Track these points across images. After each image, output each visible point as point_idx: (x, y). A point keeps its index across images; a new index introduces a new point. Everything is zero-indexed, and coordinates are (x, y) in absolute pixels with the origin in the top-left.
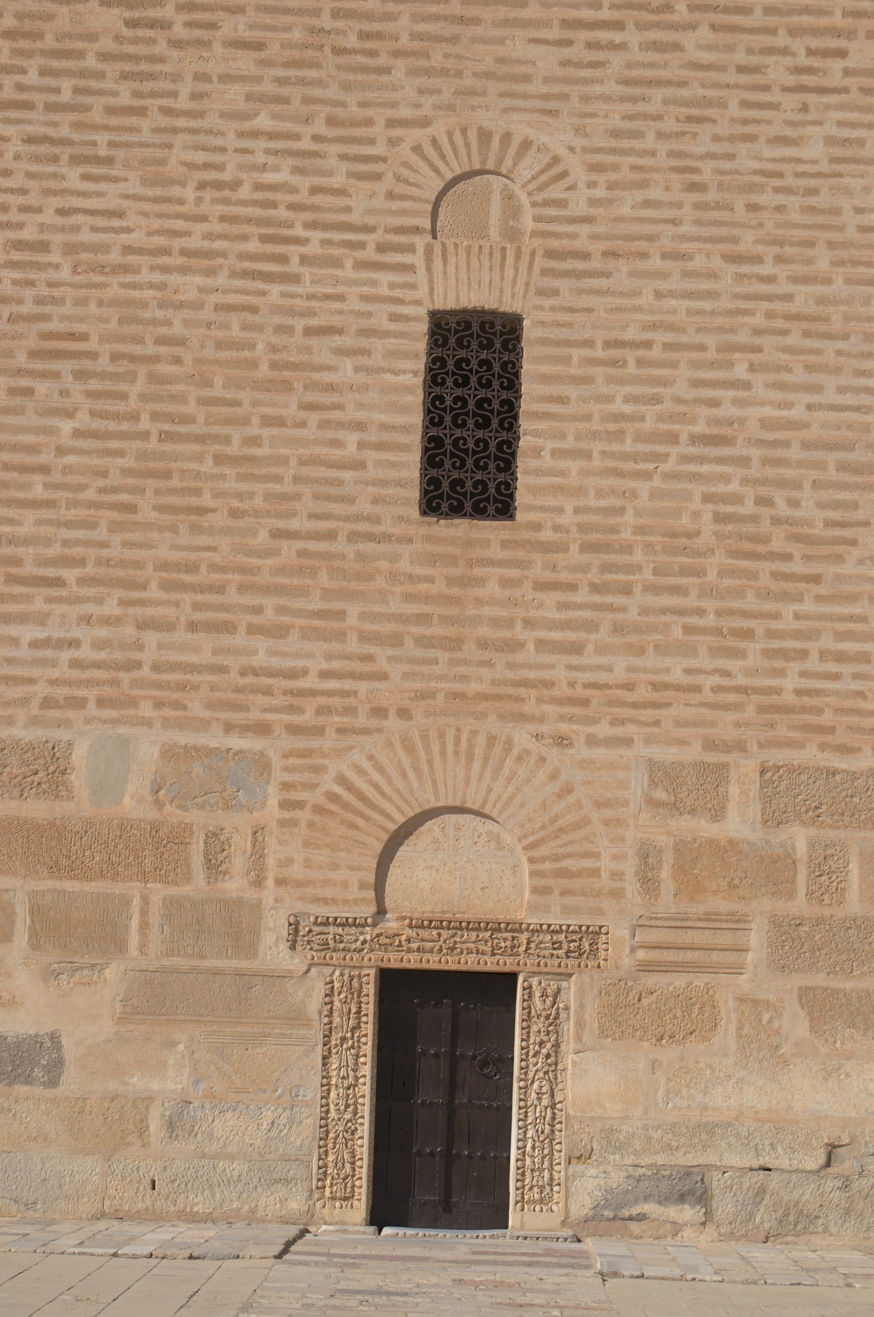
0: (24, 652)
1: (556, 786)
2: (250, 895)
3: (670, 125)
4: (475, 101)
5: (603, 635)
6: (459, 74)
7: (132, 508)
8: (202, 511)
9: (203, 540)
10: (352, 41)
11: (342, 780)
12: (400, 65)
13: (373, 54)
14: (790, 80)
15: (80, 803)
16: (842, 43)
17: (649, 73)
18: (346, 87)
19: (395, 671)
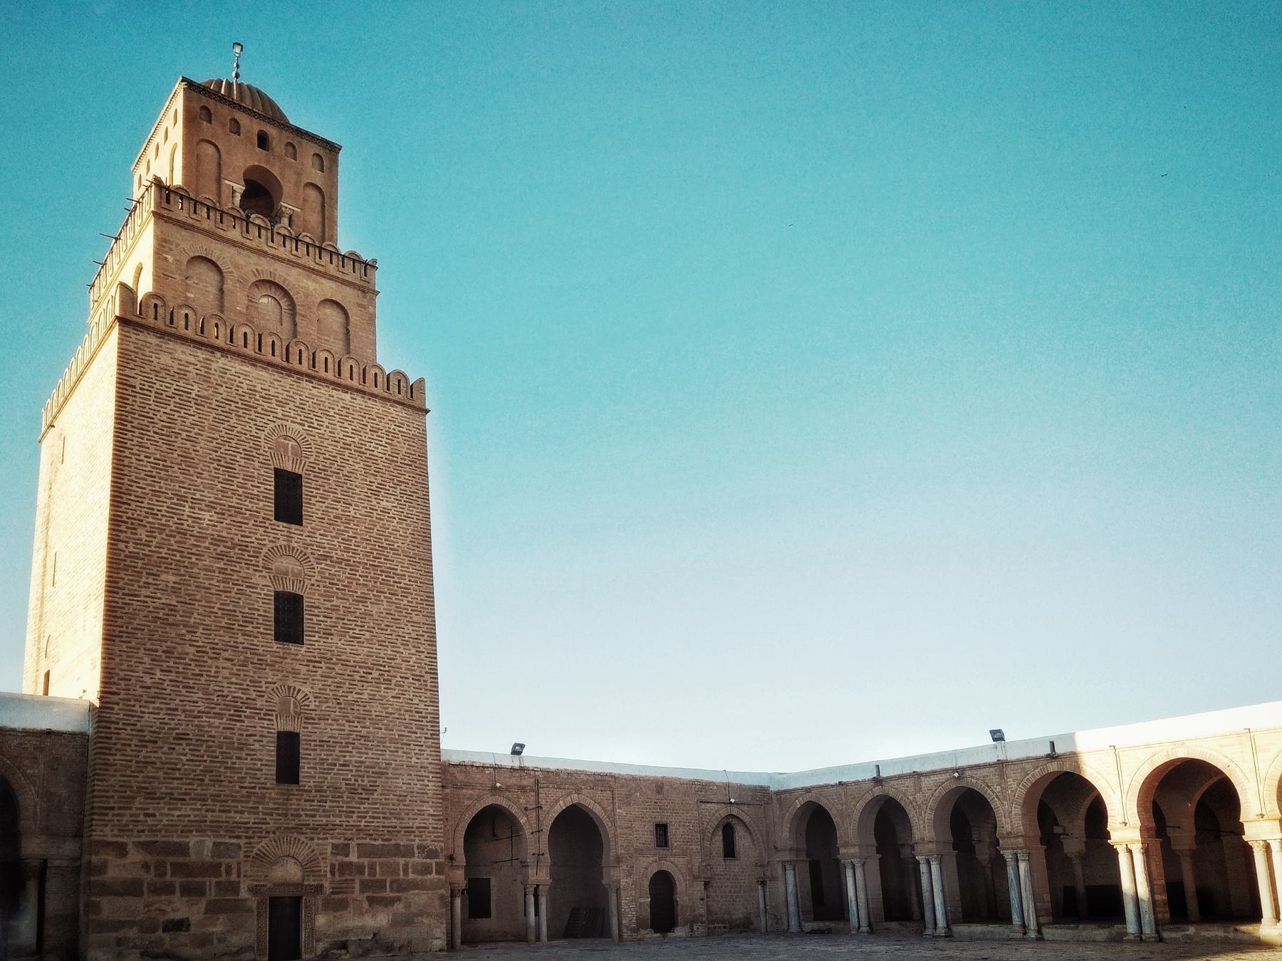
15: (193, 857)
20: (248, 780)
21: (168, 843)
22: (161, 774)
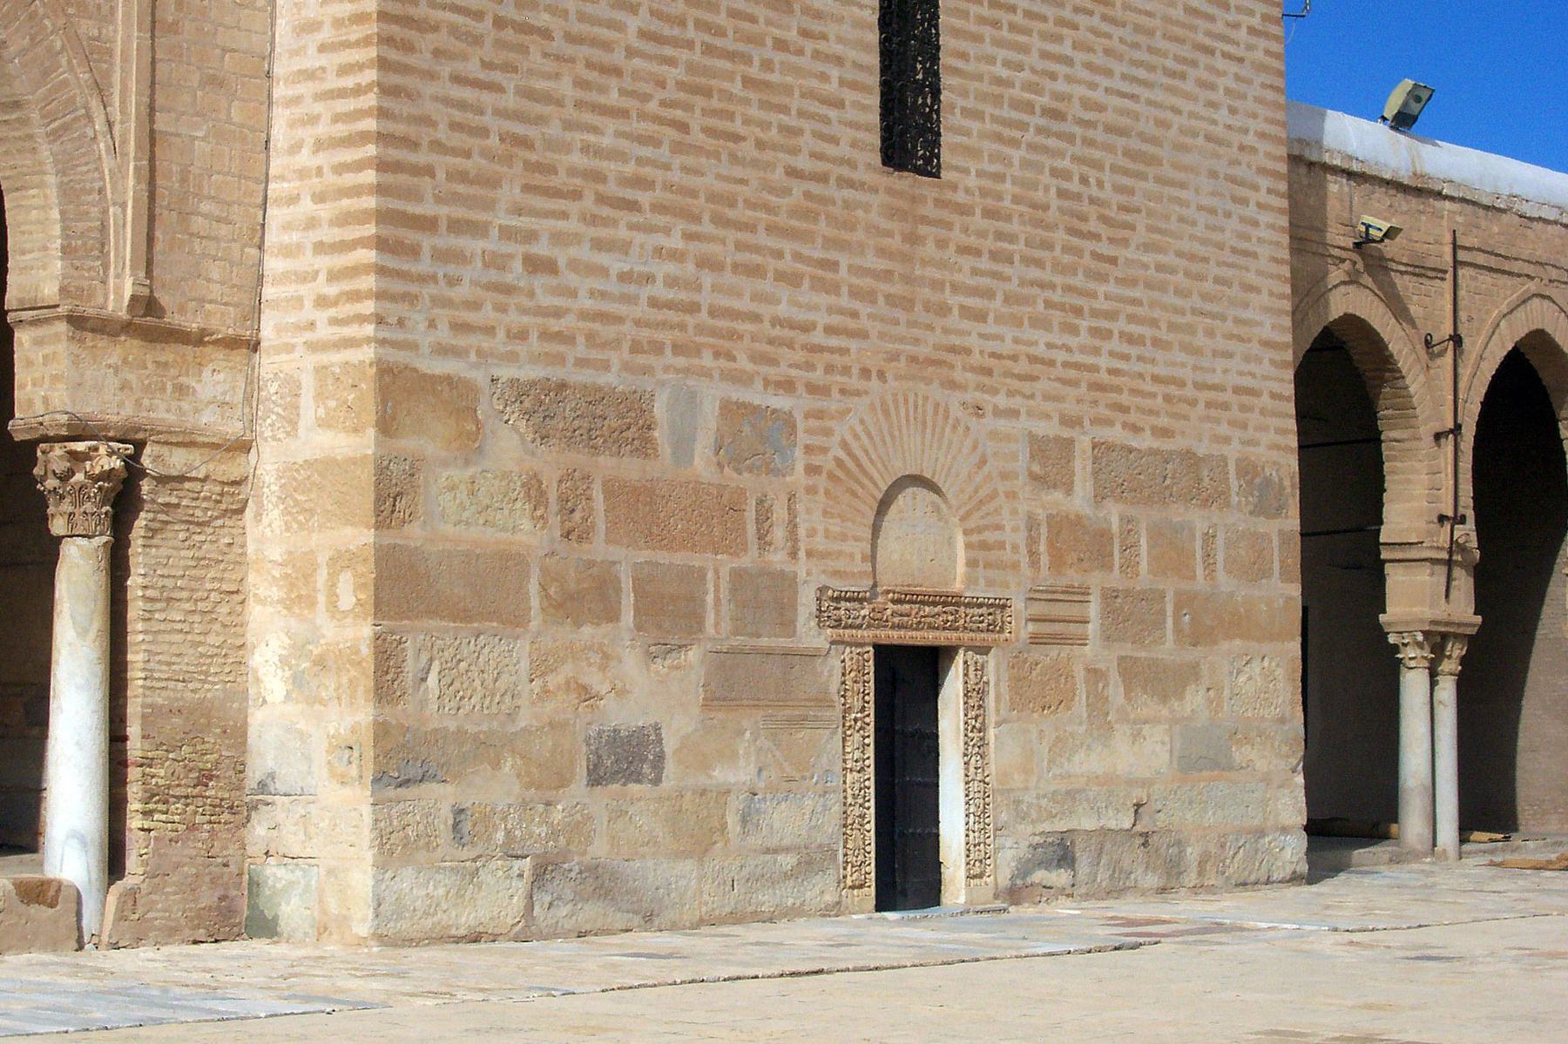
0: (613, 287)
1: (975, 458)
2: (788, 568)
5: (997, 303)
7: (683, 127)
8: (737, 138)
9: (738, 172)
11: (844, 445)
19: (874, 328)
20: (807, 141)
21: (597, 396)
22: (565, 88)
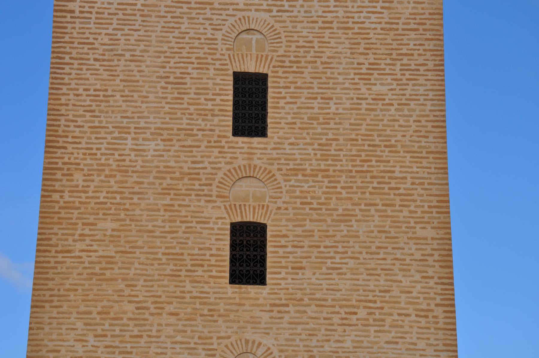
3: (303, 337)
4: (243, 330)
6: (239, 322)
10: (206, 312)
12: (221, 319)
13: (212, 316)
14: (340, 322)
16: (355, 310)
17: (297, 320)
18: (204, 326)
